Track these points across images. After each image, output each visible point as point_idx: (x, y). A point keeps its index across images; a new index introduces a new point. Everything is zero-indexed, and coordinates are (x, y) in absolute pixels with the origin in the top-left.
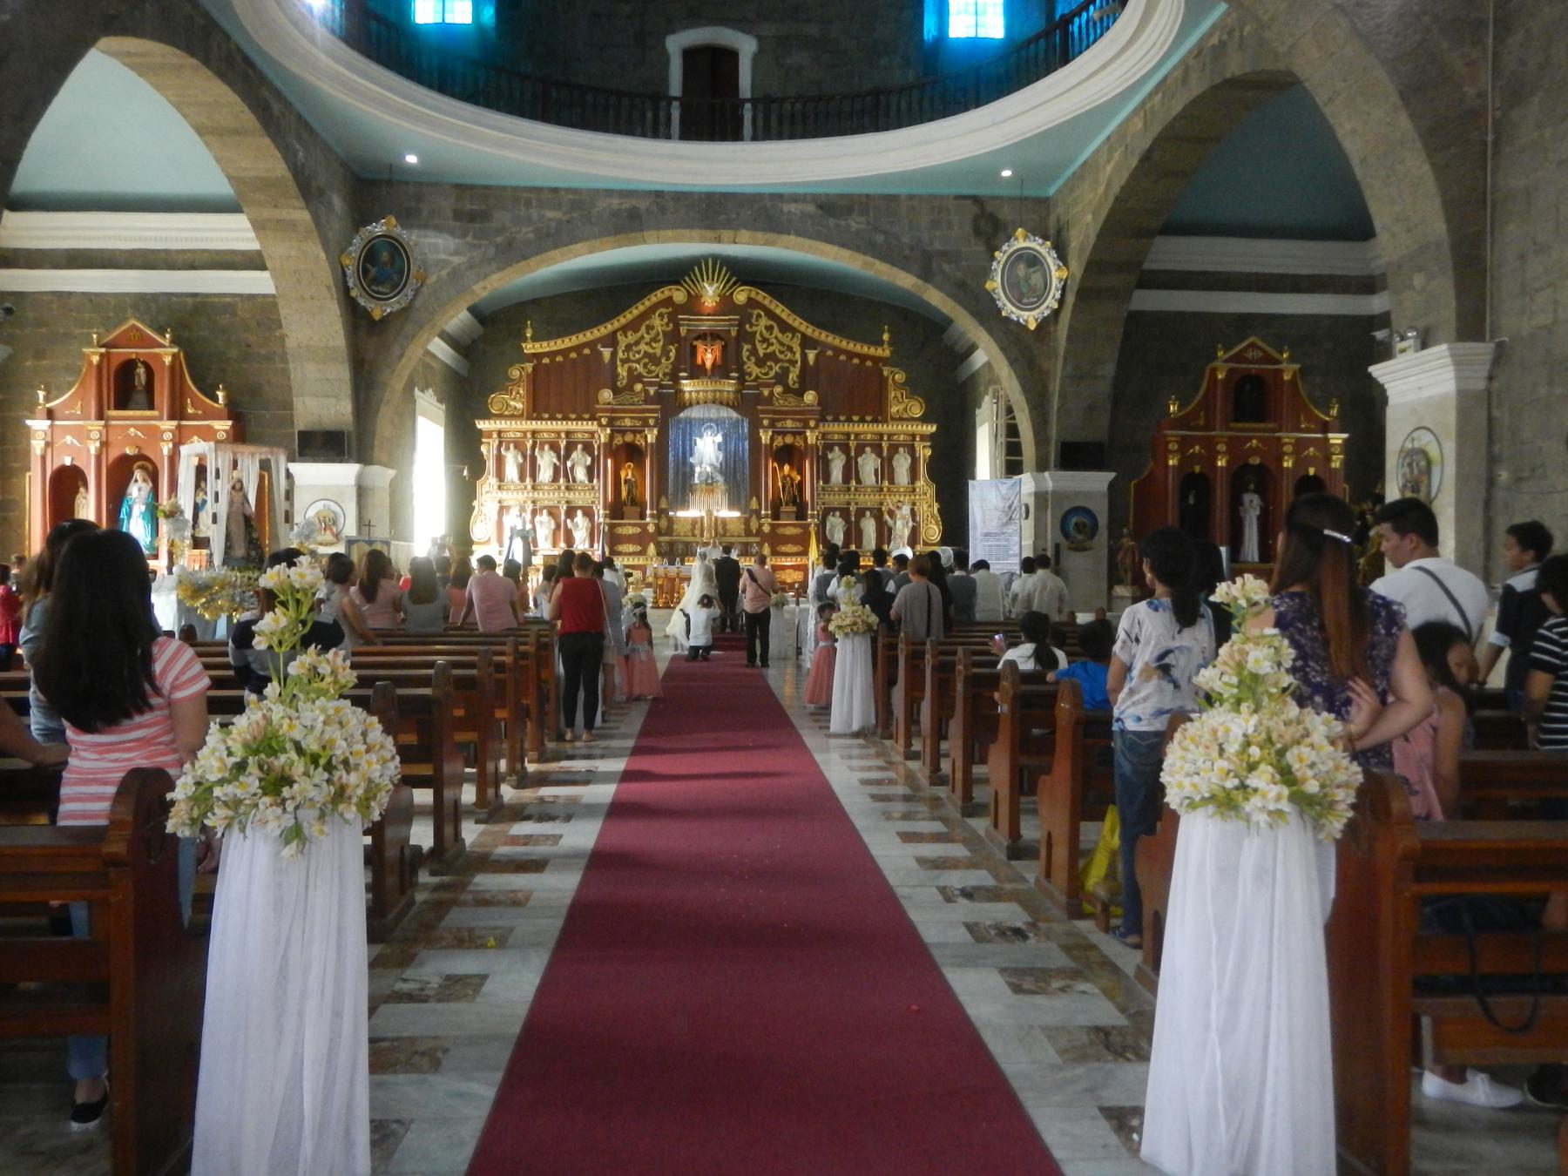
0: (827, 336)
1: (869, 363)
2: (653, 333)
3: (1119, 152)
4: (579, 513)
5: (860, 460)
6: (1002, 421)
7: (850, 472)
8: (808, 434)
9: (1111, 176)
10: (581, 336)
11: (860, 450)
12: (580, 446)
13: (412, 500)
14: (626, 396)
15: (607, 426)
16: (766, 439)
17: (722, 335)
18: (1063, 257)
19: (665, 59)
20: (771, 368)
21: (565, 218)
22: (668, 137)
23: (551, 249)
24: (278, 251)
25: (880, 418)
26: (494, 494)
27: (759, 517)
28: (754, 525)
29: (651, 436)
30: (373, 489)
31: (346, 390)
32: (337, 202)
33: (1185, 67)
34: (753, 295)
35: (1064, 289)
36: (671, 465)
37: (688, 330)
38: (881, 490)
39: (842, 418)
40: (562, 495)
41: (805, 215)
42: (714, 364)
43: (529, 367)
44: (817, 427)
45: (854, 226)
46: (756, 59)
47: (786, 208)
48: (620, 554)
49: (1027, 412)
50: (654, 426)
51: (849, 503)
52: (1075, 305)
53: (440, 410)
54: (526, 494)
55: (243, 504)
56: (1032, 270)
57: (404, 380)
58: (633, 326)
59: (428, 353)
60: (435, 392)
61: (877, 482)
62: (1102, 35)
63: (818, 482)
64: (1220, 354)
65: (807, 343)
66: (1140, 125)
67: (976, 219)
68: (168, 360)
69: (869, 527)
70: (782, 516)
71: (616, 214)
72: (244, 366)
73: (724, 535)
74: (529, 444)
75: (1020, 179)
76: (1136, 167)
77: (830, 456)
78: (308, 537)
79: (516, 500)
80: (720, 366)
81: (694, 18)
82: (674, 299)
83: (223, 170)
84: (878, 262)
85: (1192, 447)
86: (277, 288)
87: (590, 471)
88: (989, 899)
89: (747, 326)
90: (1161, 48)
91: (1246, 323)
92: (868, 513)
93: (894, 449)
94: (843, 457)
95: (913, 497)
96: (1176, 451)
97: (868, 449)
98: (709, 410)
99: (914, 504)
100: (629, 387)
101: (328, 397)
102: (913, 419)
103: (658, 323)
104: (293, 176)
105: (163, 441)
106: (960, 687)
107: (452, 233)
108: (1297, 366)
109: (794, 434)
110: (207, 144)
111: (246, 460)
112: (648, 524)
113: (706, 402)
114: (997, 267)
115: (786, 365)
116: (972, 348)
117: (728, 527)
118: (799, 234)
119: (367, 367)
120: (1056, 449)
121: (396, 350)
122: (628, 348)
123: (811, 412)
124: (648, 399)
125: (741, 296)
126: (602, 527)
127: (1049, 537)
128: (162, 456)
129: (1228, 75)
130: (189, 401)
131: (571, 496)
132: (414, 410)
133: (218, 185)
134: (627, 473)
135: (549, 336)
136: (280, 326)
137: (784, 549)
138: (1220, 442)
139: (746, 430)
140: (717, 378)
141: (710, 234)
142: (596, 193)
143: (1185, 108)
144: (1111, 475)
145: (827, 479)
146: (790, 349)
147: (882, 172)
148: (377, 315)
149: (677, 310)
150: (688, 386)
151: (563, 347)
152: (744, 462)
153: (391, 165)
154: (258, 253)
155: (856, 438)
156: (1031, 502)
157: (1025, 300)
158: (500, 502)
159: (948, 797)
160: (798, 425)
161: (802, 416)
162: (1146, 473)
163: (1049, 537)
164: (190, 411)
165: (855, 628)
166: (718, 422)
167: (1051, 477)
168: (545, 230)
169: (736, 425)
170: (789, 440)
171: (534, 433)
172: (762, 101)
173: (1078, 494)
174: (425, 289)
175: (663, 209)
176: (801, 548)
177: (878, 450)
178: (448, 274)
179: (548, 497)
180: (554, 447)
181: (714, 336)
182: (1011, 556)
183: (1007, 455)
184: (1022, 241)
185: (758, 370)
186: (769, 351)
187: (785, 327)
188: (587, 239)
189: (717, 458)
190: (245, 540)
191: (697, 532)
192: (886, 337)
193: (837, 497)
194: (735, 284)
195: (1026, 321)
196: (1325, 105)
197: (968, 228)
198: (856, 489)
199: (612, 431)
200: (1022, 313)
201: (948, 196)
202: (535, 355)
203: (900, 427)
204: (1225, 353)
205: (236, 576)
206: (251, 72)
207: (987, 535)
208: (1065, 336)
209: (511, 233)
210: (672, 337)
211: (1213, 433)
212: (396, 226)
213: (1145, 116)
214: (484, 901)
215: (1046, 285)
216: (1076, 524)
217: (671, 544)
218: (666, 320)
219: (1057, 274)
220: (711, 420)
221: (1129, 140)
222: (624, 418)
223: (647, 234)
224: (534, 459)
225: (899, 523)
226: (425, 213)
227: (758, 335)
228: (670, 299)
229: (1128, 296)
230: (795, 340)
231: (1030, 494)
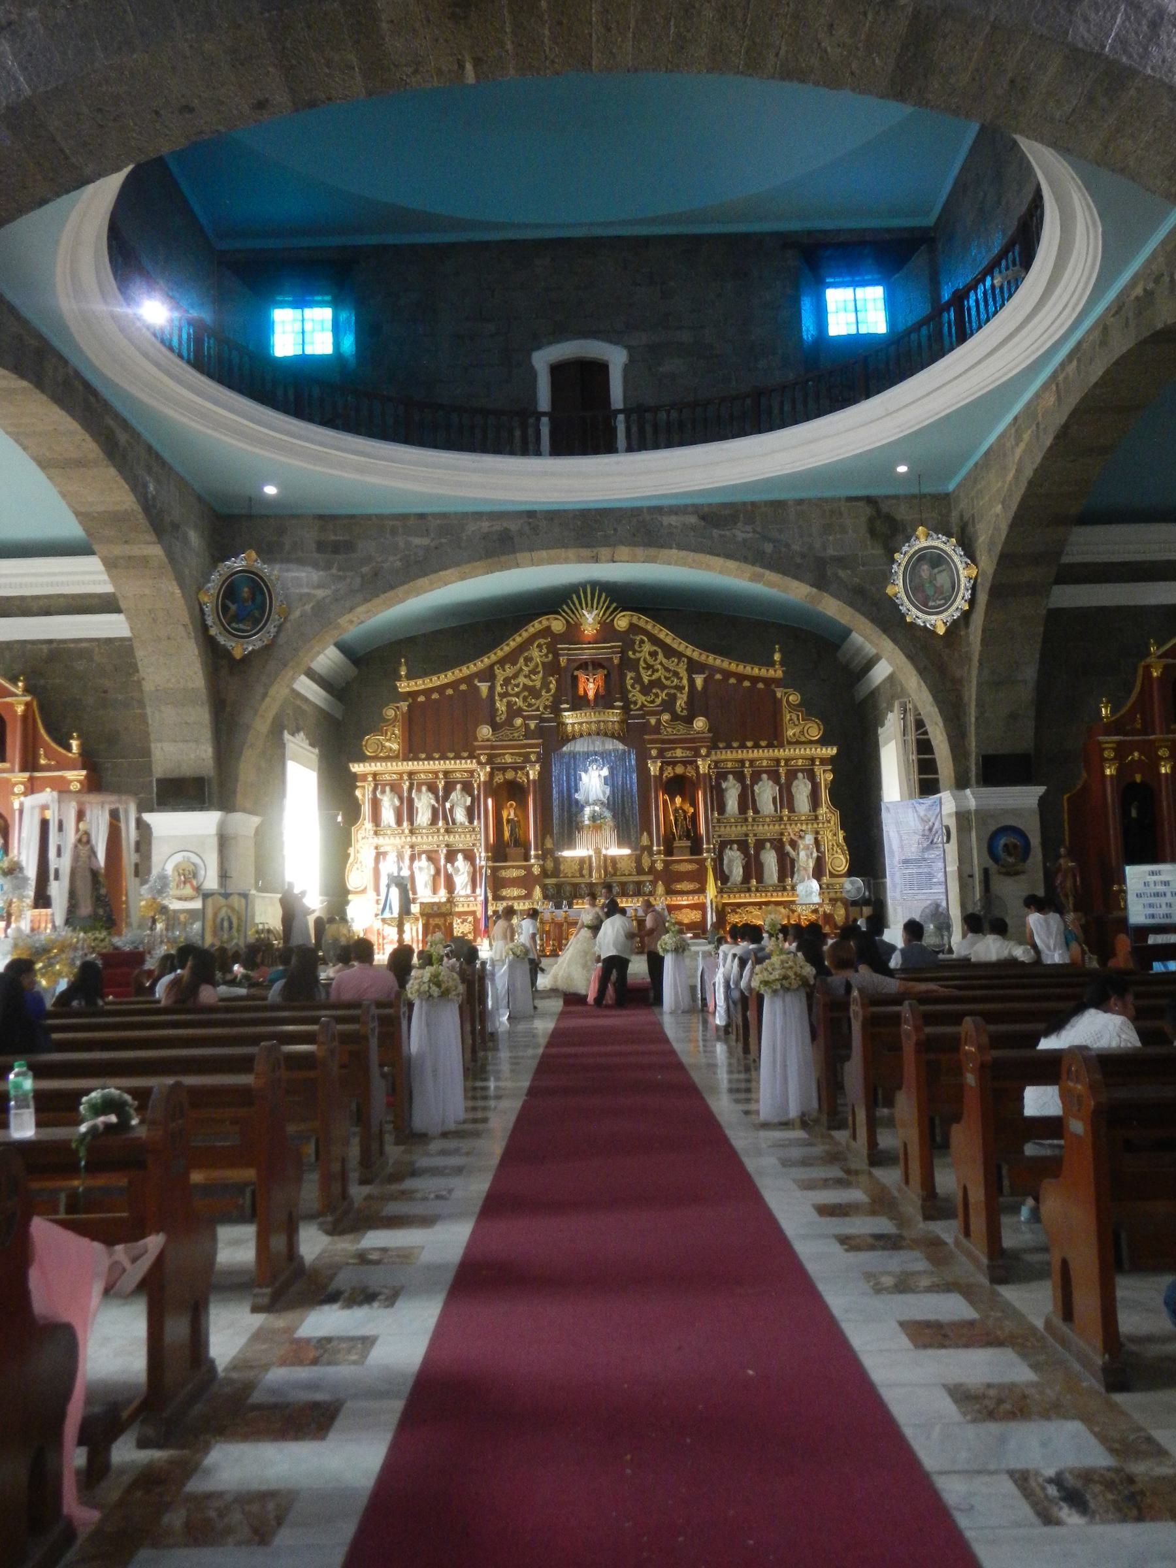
0: (715, 659)
1: (761, 685)
2: (532, 665)
3: (1029, 432)
4: (460, 856)
5: (756, 788)
6: (912, 737)
7: (747, 801)
10: (457, 671)
11: (756, 777)
12: (459, 786)
13: (282, 850)
14: (506, 731)
15: (486, 763)
16: (655, 770)
17: (605, 664)
18: (970, 554)
20: (657, 695)
21: (433, 544)
22: (538, 453)
23: (420, 577)
24: (133, 589)
25: (775, 743)
26: (370, 839)
27: (651, 854)
29: (533, 775)
30: (235, 838)
31: (206, 733)
32: (194, 537)
33: (1103, 328)
34: (635, 620)
35: (974, 589)
36: (555, 803)
37: (568, 660)
38: (781, 819)
39: (735, 744)
40: (441, 838)
42: (596, 695)
43: (404, 706)
44: (708, 755)
45: (740, 536)
46: (626, 369)
47: (666, 520)
48: (503, 898)
49: (941, 724)
51: (747, 835)
52: (989, 605)
53: (313, 754)
54: (403, 838)
55: (90, 858)
56: (936, 570)
57: (269, 721)
58: (511, 658)
59: (298, 695)
60: (307, 736)
61: (776, 810)
62: (1003, 305)
63: (712, 814)
65: (694, 667)
66: (1053, 399)
67: (871, 520)
68: (20, 709)
69: (770, 859)
70: (675, 851)
71: (485, 537)
73: (615, 874)
74: (406, 786)
75: (916, 475)
76: (1051, 448)
77: (724, 785)
78: (160, 892)
79: (394, 845)
80: (603, 697)
81: (560, 333)
82: (553, 628)
83: (70, 505)
84: (767, 573)
85: (1132, 754)
86: (132, 629)
87: (470, 813)
89: (630, 653)
90: (1074, 309)
92: (768, 845)
93: (792, 775)
94: (738, 785)
95: (815, 826)
96: (1111, 760)
97: (765, 776)
98: (593, 743)
99: (817, 833)
100: (509, 722)
101: (187, 741)
102: (811, 742)
103: (537, 655)
104: (143, 510)
105: (14, 794)
106: (970, 1079)
107: (316, 566)
109: (685, 763)
110: (50, 478)
111: (95, 811)
112: (533, 865)
113: (590, 734)
114: (898, 570)
115: (673, 691)
116: (871, 663)
117: (619, 866)
119: (228, 709)
120: (976, 764)
122: (507, 681)
123: (702, 740)
125: (622, 622)
126: (484, 871)
127: (976, 861)
129: (1159, 326)
130: (42, 752)
131: (451, 839)
134: (509, 813)
135: (425, 674)
136: (138, 671)
137: (679, 887)
138: (1161, 747)
139: (633, 762)
140: (598, 709)
141: (586, 552)
142: (465, 515)
143: (1107, 372)
144: (1040, 790)
145: (722, 808)
146: (676, 674)
148: (238, 654)
149: (554, 640)
150: (570, 718)
151: (439, 683)
152: (632, 796)
153: (250, 499)
154: (114, 594)
155: (751, 766)
156: (952, 823)
157: (931, 604)
158: (376, 848)
159: (957, 1243)
160: (688, 753)
161: (693, 744)
162: (1079, 787)
163: (976, 861)
164: (43, 762)
165: (785, 983)
166: (604, 756)
167: (973, 794)
168: (413, 557)
169: (622, 756)
170: (679, 770)
171: (411, 774)
173: (1006, 812)
174: (288, 625)
175: (535, 530)
176: (698, 886)
177: (774, 776)
178: (313, 608)
179: (426, 841)
180: (432, 789)
181: (597, 665)
182: (936, 884)
183: (920, 773)
184: (923, 540)
185: (644, 698)
186: (654, 677)
187: (670, 652)
188: (457, 564)
189: (604, 793)
190: (92, 897)
191: (585, 872)
192: (777, 657)
193: (734, 828)
194: (615, 609)
195: (934, 626)
198: (754, 820)
199: (492, 769)
200: (929, 617)
201: (840, 499)
202: (410, 694)
203: (797, 750)
204: (1158, 649)
205: (78, 938)
206: (92, 399)
207: (906, 862)
208: (979, 639)
209: (377, 562)
210: (552, 668)
211: (1152, 737)
212: (256, 561)
213: (1058, 391)
215: (954, 586)
216: (1006, 846)
217: (559, 886)
218: (545, 651)
219: (966, 573)
220: (596, 754)
222: (504, 754)
224: (411, 802)
225: (802, 854)
226: (287, 547)
227: (642, 663)
230: (681, 665)
231: (949, 815)
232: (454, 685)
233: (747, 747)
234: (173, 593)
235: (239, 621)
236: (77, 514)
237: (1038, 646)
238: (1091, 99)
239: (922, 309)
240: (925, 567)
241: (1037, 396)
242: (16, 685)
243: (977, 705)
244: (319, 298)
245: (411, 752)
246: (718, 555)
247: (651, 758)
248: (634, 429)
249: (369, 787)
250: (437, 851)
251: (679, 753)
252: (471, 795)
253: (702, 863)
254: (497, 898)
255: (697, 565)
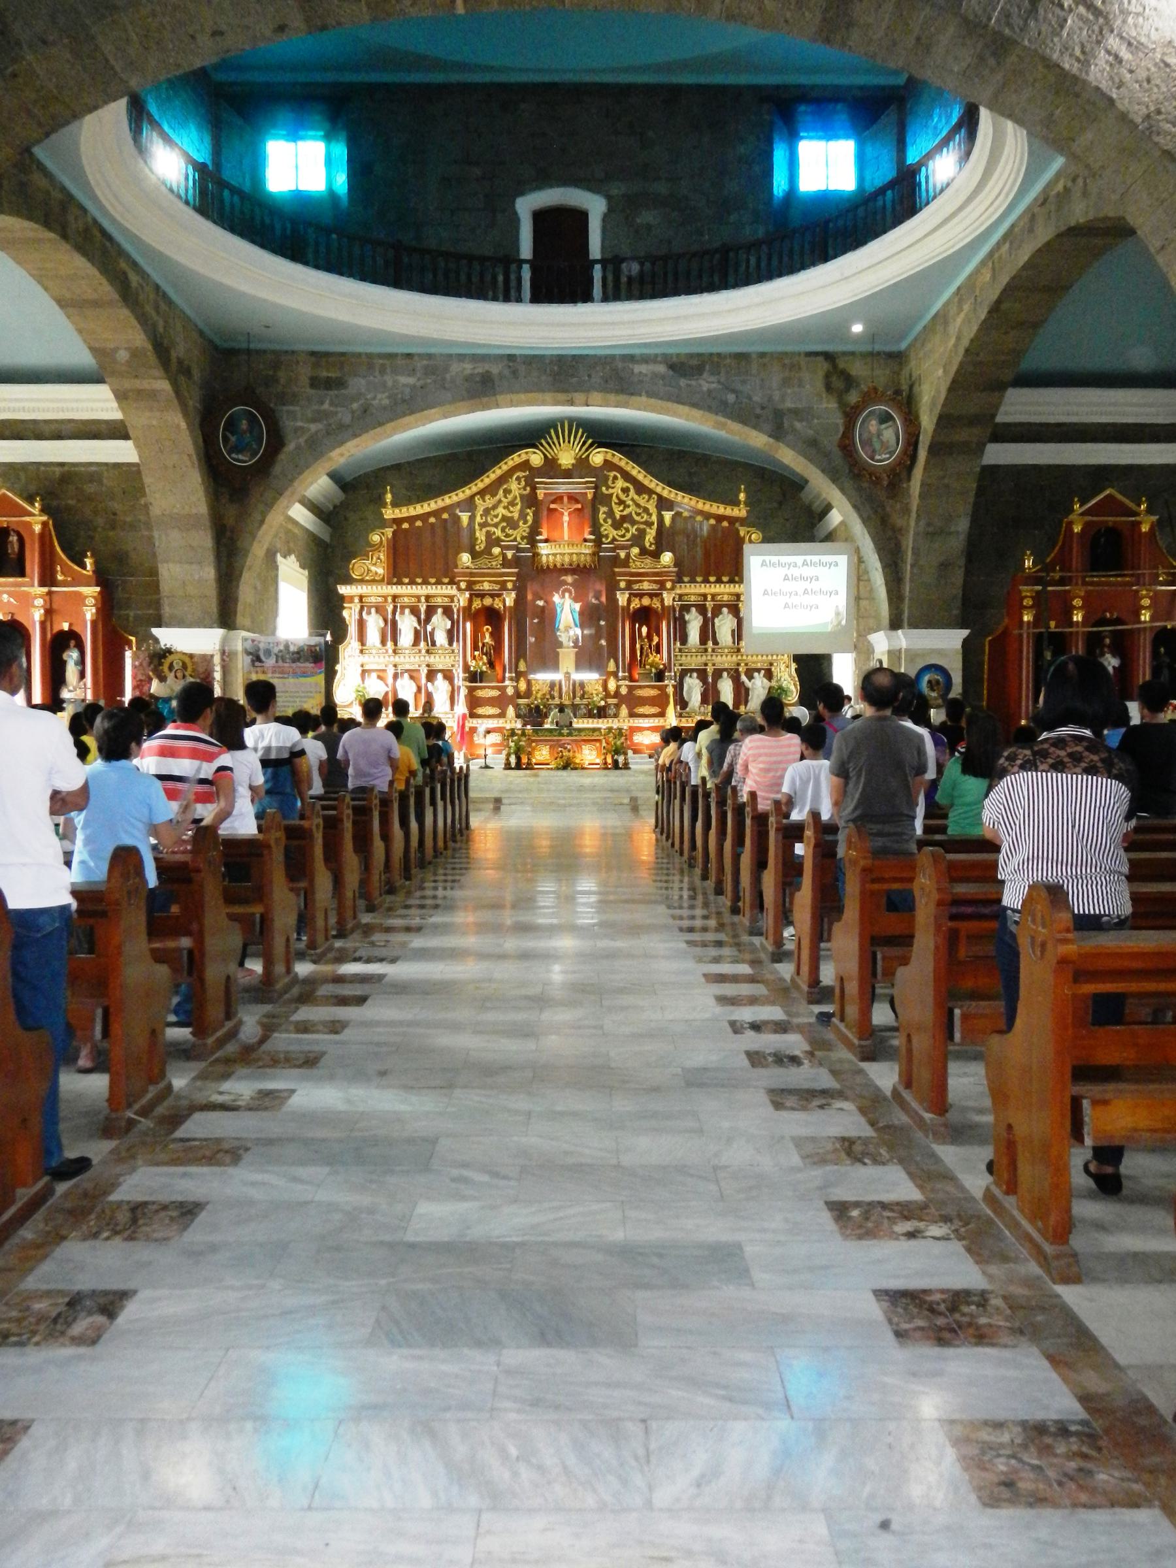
1: (725, 524)
2: (510, 497)
4: (440, 676)
5: (716, 620)
7: (707, 633)
8: (665, 594)
9: (960, 331)
10: (439, 500)
11: (717, 611)
12: (440, 611)
15: (466, 590)
19: (515, 221)
20: (627, 530)
21: (419, 384)
22: (519, 300)
24: (139, 420)
25: (737, 579)
27: (617, 679)
28: (612, 685)
29: (510, 599)
31: (210, 557)
33: (1031, 216)
34: (609, 457)
39: (699, 579)
41: (655, 375)
43: (389, 532)
44: (673, 588)
45: (705, 387)
46: (605, 218)
47: (638, 368)
48: (479, 716)
49: (880, 570)
50: (512, 590)
51: (706, 665)
52: (927, 462)
56: (883, 426)
58: (491, 490)
64: (1077, 506)
65: (664, 504)
67: (827, 376)
68: (37, 528)
71: (467, 379)
72: (111, 533)
74: (390, 608)
75: (871, 336)
76: (985, 321)
77: (687, 617)
81: (544, 180)
83: (85, 341)
84: (729, 422)
87: (451, 635)
88: (776, 1032)
91: (1101, 475)
94: (700, 618)
97: (725, 610)
99: (771, 664)
100: (487, 551)
103: (515, 487)
108: (1154, 518)
109: (651, 596)
110: (69, 317)
112: (506, 687)
115: (642, 526)
116: (828, 508)
117: (586, 689)
118: (650, 395)
119: (228, 534)
121: (257, 516)
122: (487, 512)
124: (506, 563)
128: (34, 623)
129: (1073, 224)
130: (59, 568)
131: (432, 659)
132: (277, 576)
133: (83, 358)
135: (409, 502)
136: (144, 495)
137: (641, 710)
141: (561, 396)
142: (450, 356)
144: (965, 633)
145: (684, 639)
146: (646, 510)
147: (712, 334)
149: (532, 474)
155: (713, 599)
160: (655, 586)
164: (60, 577)
167: (905, 635)
170: (646, 601)
171: (395, 597)
172: (612, 262)
173: (933, 651)
175: (515, 373)
178: (306, 441)
180: (415, 611)
186: (625, 513)
187: (641, 489)
191: (556, 694)
192: (742, 496)
196: (1158, 252)
197: (820, 384)
198: (713, 650)
201: (799, 354)
206: (108, 244)
213: (993, 269)
214: (304, 1028)
216: (929, 682)
218: (523, 483)
221: (977, 293)
223: (500, 398)
224: (394, 623)
226: (282, 381)
227: (614, 499)
228: (527, 461)
229: (980, 450)
232: (436, 513)
233: (709, 582)
234: (178, 426)
235: (239, 452)
236: (91, 349)
237: (971, 500)
238: (981, 58)
239: (884, 172)
240: (874, 422)
241: (977, 271)
242: (32, 504)
243: (913, 553)
244: (311, 133)
245: (396, 574)
246: (683, 404)
247: (621, 590)
248: (610, 278)
249: (356, 607)
250: (418, 671)
251: (646, 586)
252: (451, 618)
253: (663, 689)
254: (473, 715)
255: (666, 412)
